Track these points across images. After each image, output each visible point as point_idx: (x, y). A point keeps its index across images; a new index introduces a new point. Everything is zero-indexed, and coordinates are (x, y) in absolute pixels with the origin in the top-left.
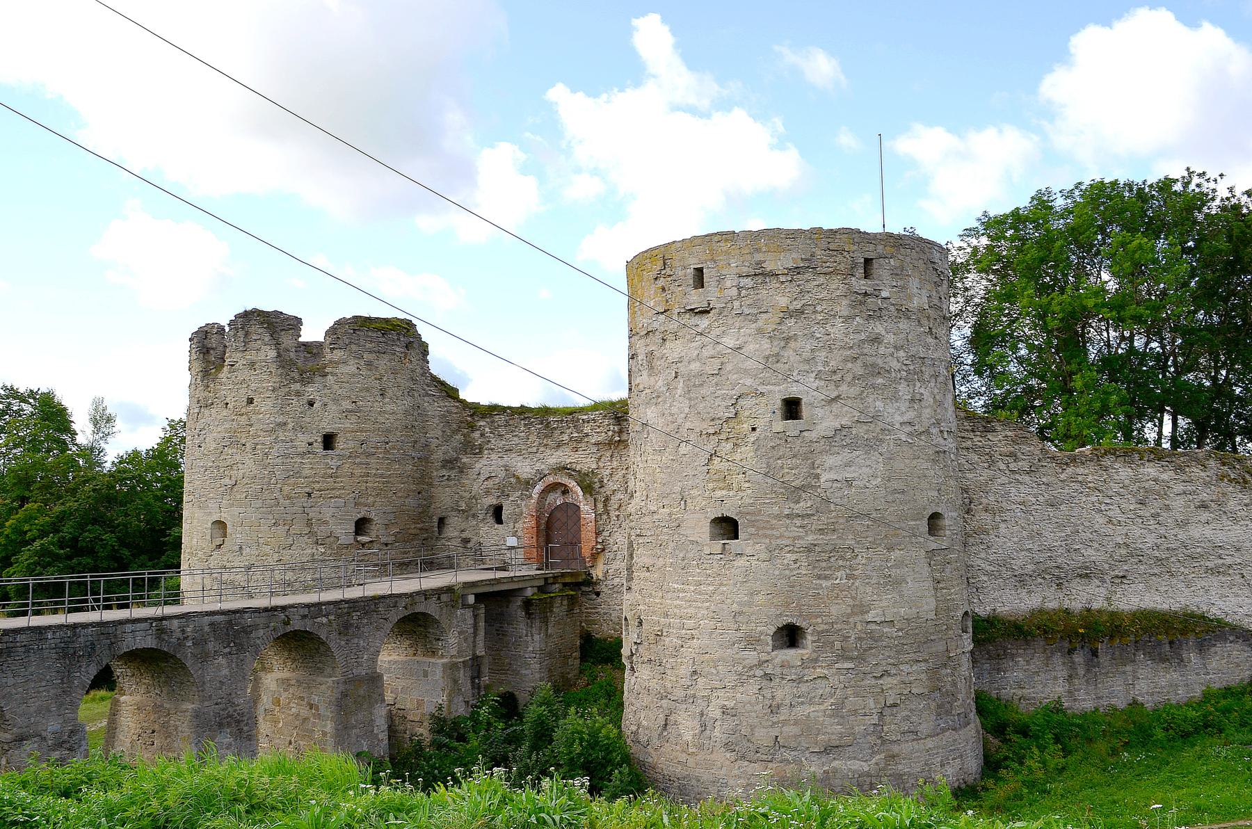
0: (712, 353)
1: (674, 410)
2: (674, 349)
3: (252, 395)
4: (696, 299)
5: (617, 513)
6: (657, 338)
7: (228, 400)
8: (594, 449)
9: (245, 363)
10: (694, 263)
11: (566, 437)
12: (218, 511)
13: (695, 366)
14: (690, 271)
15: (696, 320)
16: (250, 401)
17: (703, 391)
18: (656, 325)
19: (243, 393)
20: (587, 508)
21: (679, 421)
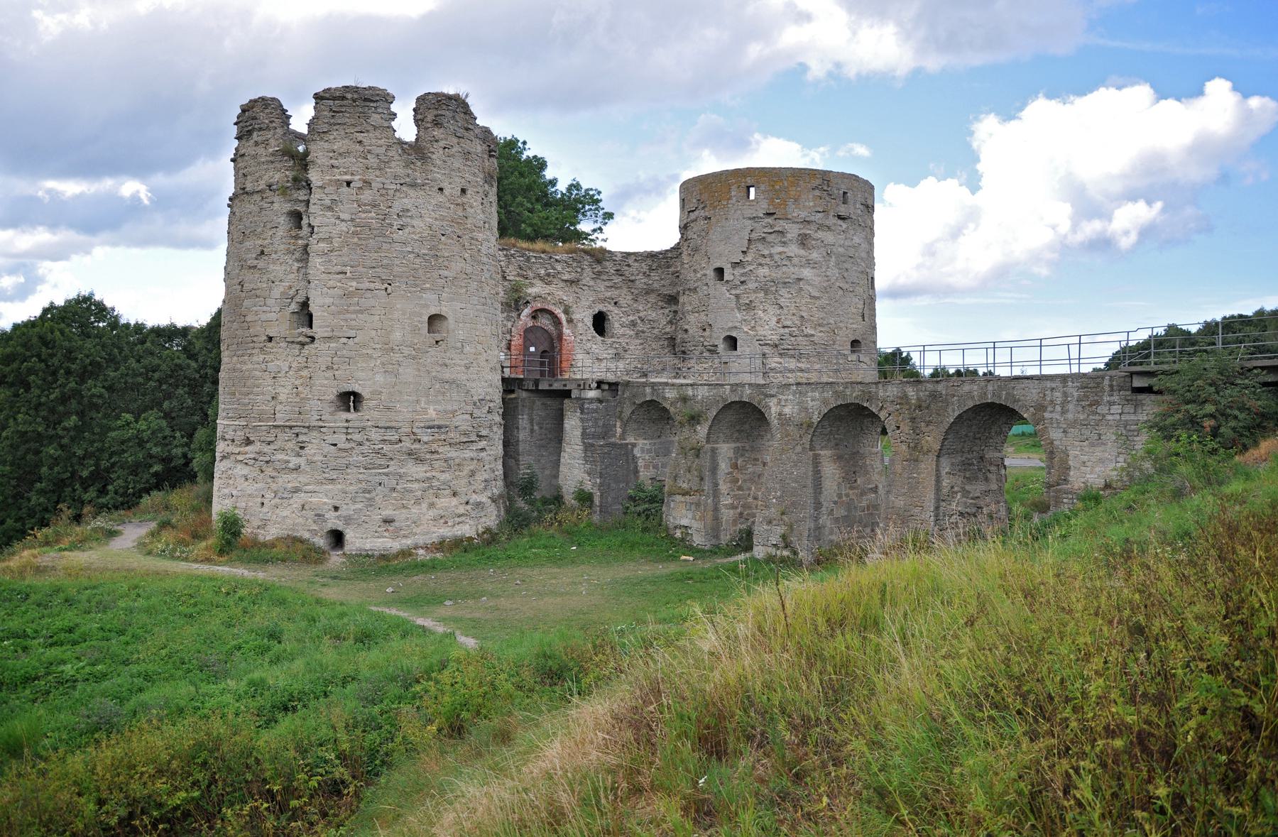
0: (850, 244)
1: (828, 274)
2: (829, 237)
3: (467, 186)
4: (843, 210)
5: (580, 337)
6: (813, 227)
7: (442, 186)
8: (562, 284)
9: (460, 150)
10: (843, 188)
11: (542, 272)
12: (437, 303)
13: (841, 250)
14: (841, 192)
15: (840, 222)
16: (463, 191)
17: (846, 265)
18: (812, 218)
19: (458, 183)
20: (568, 331)
21: (833, 281)
